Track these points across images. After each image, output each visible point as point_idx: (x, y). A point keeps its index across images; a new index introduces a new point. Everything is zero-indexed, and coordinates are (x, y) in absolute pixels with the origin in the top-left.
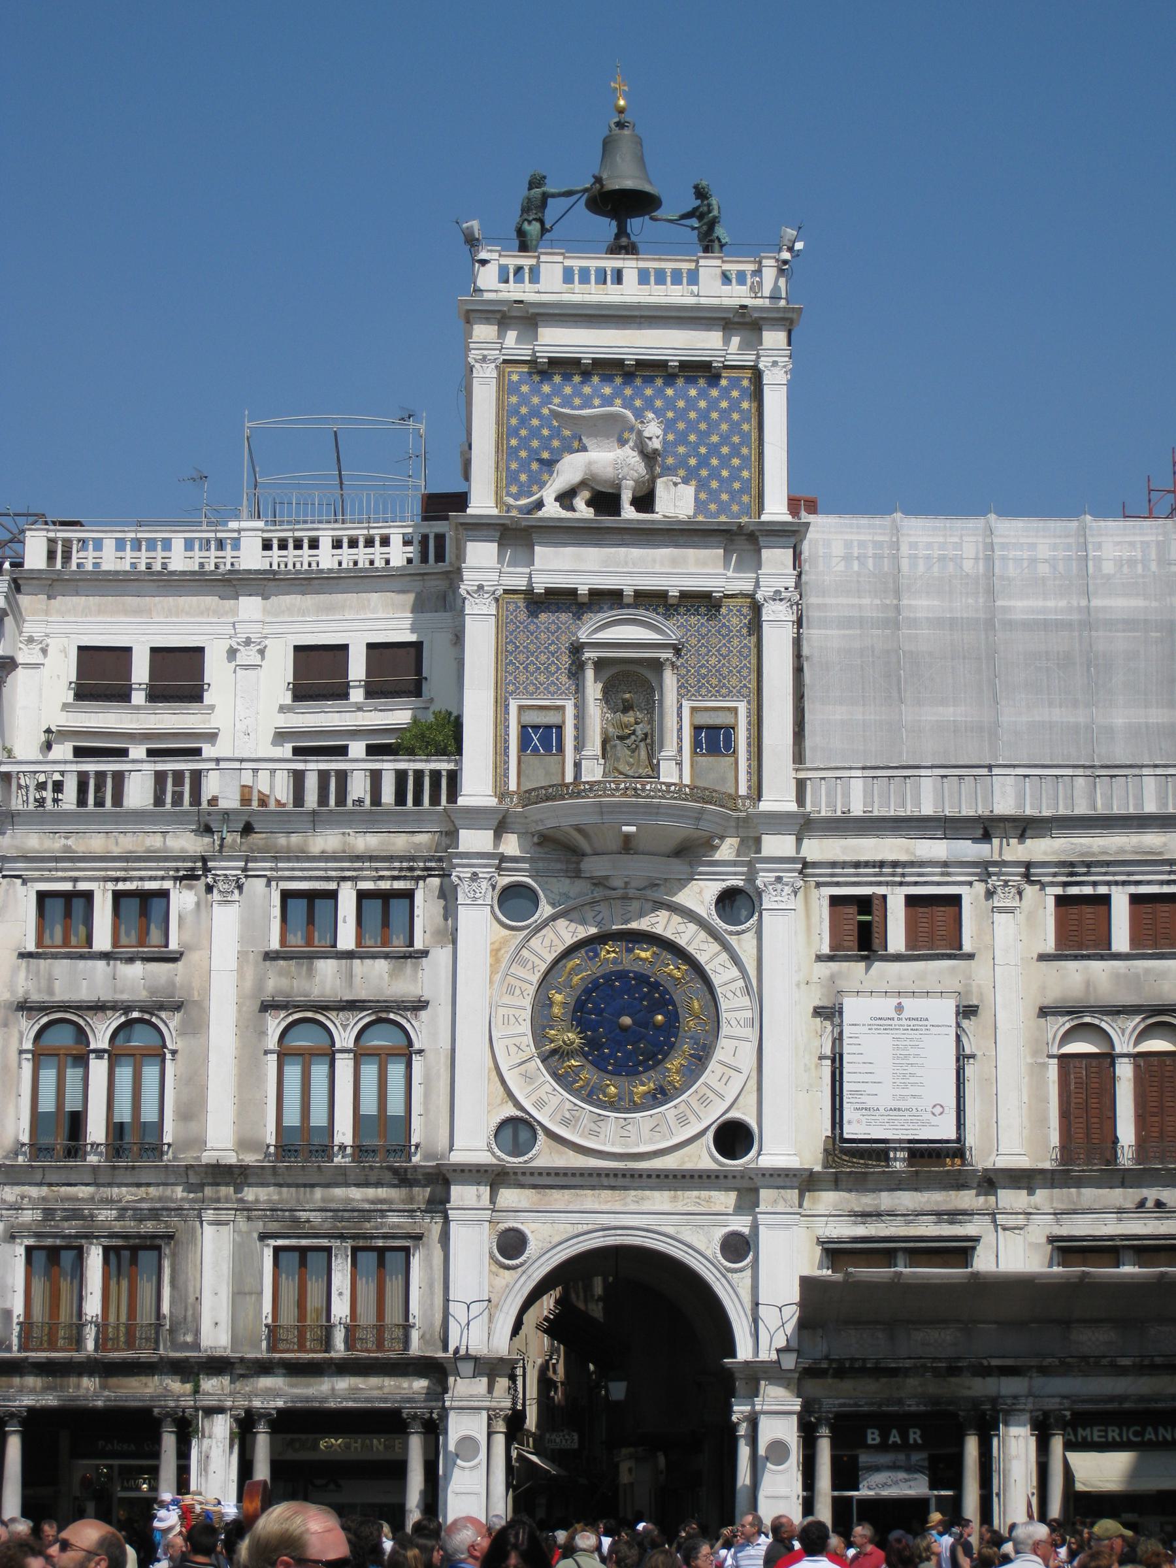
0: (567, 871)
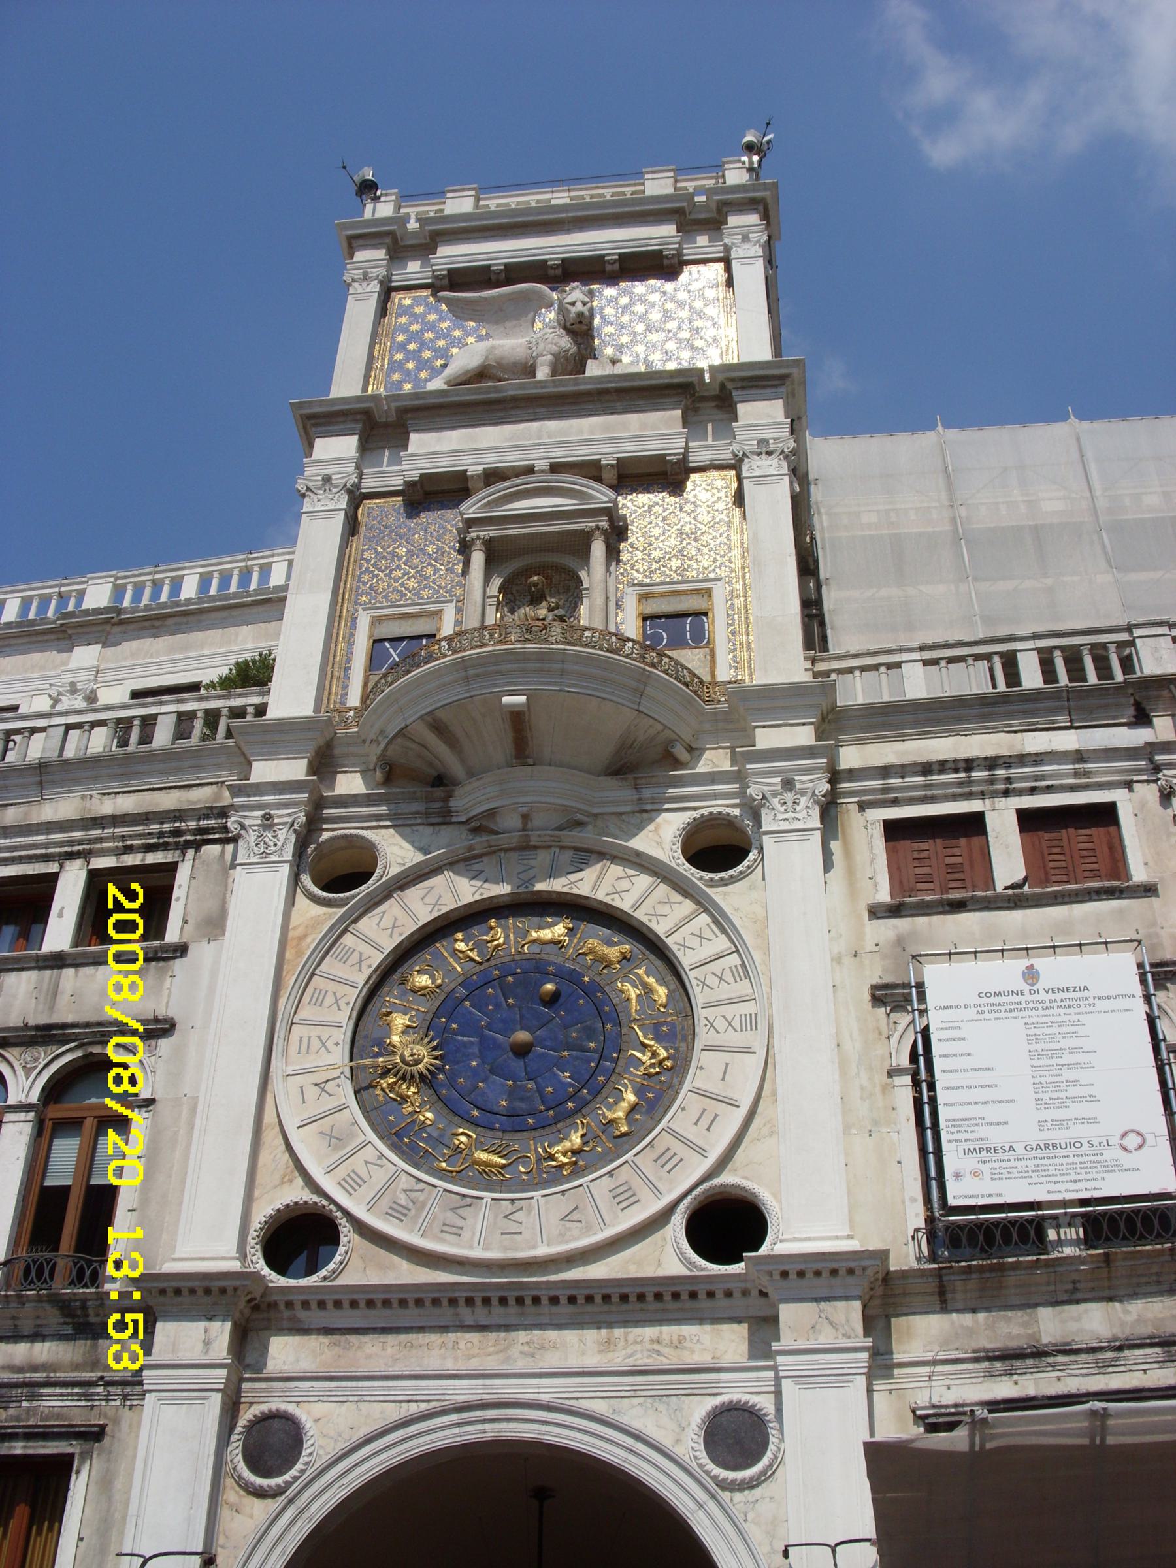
0: (427, 814)
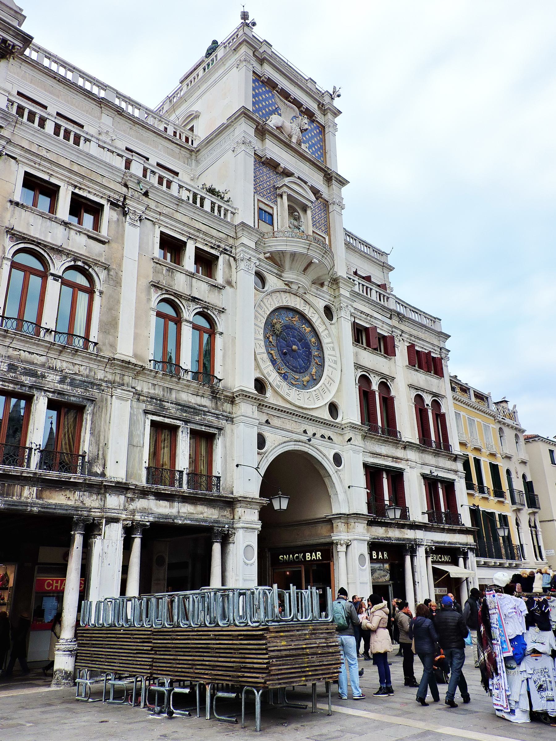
0: (277, 274)
